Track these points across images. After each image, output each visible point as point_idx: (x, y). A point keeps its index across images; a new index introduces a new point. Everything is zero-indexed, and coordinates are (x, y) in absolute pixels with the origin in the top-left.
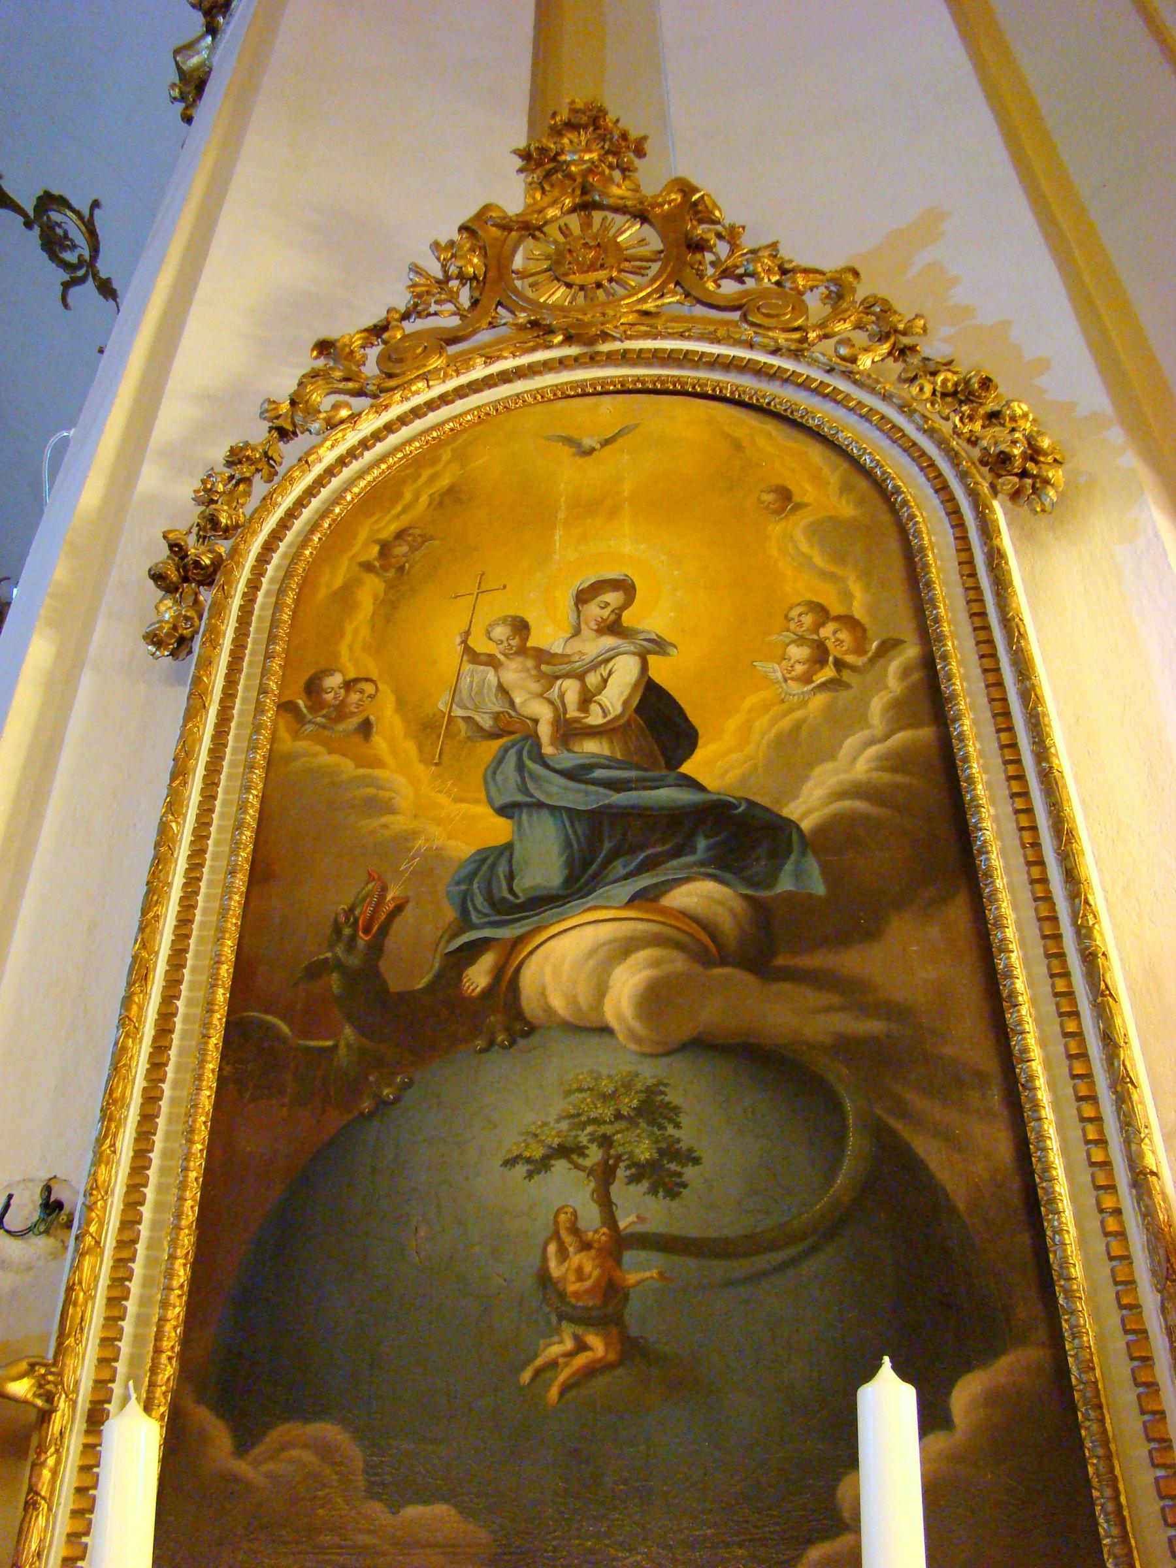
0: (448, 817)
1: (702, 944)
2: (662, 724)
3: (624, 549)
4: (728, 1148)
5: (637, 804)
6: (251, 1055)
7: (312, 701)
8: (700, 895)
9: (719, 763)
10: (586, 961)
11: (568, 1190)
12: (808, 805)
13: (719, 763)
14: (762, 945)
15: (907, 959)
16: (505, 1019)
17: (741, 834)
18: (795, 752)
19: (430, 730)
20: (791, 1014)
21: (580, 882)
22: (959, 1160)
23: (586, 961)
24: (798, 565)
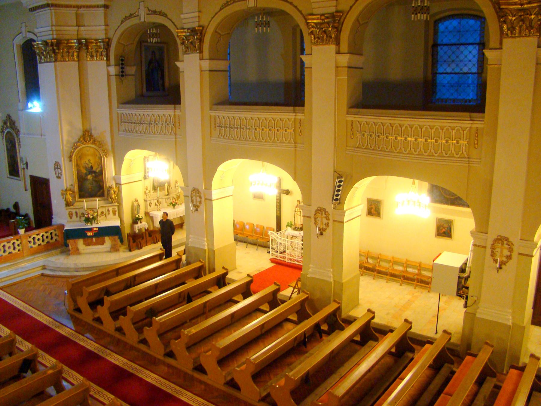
0: (84, 171)
1: (93, 176)
2: (92, 167)
3: (90, 158)
4: (94, 184)
5: (91, 171)
6: (79, 180)
7: (78, 165)
8: (93, 175)
9: (94, 169)
10: (90, 177)
11: (89, 185)
12: (97, 171)
13: (94, 169)
14: (96, 177)
15: (100, 177)
16: (87, 179)
17: (95, 172)
18: (97, 169)
19: (83, 167)
20: (97, 179)
21: (89, 174)
22: (101, 184)
23: (90, 177)
24: (97, 160)
